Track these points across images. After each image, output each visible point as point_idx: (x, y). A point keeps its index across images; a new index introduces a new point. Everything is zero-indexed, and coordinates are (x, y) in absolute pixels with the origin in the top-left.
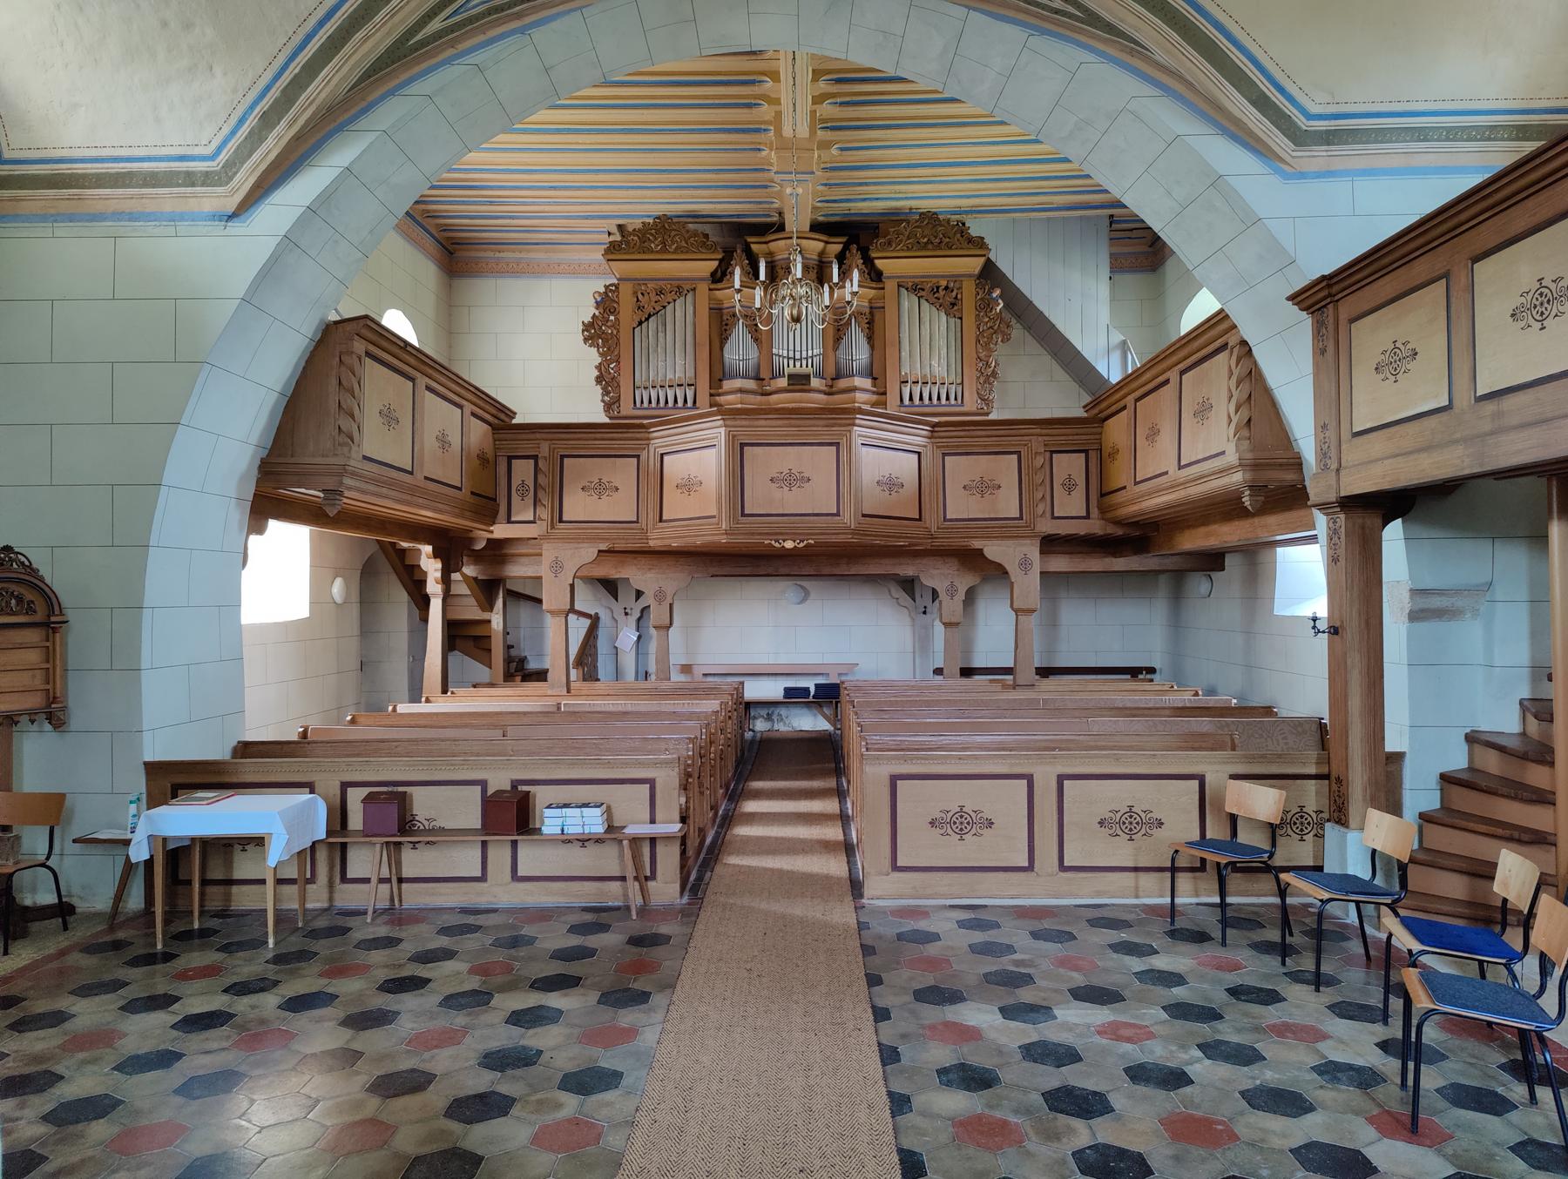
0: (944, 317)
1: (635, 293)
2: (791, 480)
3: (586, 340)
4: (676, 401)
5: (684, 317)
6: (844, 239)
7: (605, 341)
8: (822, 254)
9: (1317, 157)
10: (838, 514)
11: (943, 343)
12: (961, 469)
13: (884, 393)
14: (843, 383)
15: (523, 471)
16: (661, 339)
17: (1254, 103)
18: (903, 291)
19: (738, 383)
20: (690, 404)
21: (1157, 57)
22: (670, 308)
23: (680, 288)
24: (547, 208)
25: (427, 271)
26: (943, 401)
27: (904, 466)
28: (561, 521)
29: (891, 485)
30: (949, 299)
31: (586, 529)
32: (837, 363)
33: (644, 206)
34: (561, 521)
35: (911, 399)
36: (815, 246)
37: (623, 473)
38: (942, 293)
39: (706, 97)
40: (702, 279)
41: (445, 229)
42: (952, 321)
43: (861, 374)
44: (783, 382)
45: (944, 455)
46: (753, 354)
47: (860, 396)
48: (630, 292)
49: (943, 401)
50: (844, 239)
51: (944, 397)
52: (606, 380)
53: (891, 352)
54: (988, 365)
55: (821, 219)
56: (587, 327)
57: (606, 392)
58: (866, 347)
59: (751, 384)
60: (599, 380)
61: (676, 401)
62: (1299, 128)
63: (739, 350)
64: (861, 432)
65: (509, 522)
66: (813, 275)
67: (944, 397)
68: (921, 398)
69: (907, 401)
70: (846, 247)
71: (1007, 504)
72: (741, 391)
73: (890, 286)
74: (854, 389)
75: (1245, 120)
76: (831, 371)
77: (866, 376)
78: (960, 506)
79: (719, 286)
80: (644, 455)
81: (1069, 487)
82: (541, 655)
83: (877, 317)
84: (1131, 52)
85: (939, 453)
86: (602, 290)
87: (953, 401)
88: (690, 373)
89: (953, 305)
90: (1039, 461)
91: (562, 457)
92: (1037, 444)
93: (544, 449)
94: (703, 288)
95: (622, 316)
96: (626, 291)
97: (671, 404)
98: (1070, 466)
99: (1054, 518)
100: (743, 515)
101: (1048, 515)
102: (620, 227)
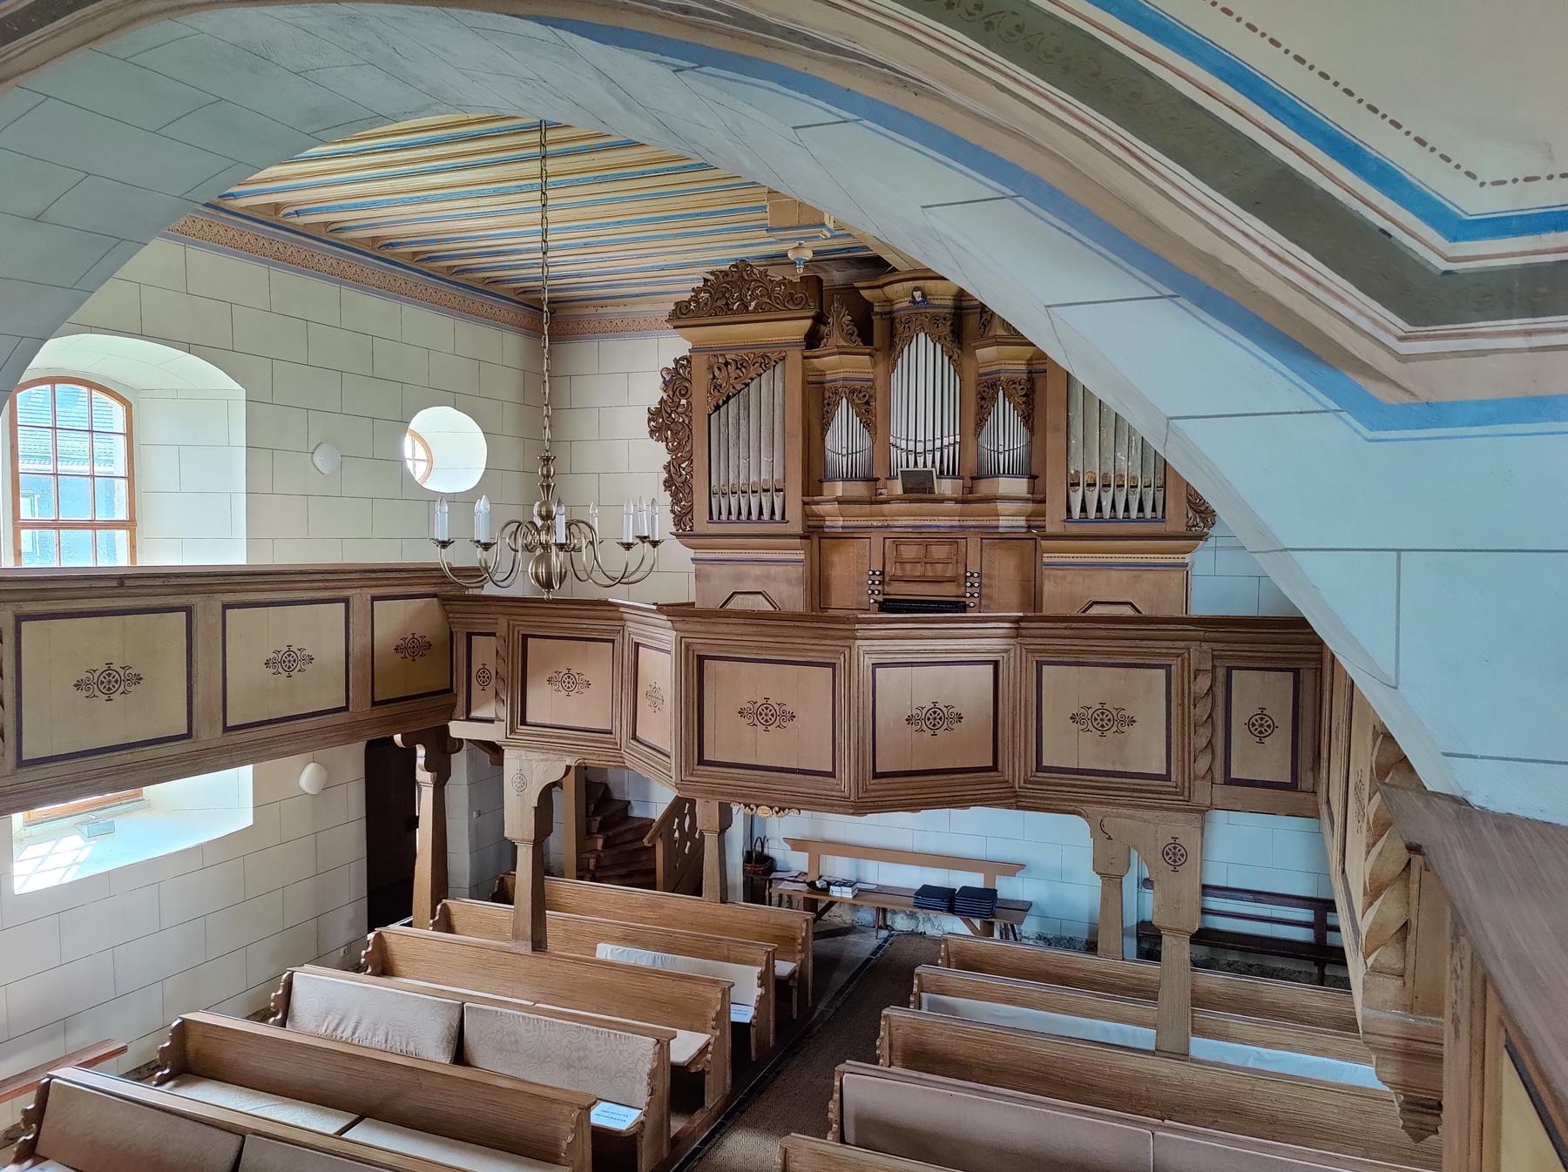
1: (710, 368)
2: (767, 715)
3: (652, 433)
5: (774, 397)
7: (675, 434)
9: (1500, 351)
10: (832, 775)
12: (1069, 688)
13: (1043, 501)
14: (985, 487)
15: (485, 652)
17: (1254, 205)
19: (839, 489)
20: (777, 517)
22: (752, 385)
23: (766, 358)
25: (502, 348)
26: (1134, 513)
27: (967, 687)
28: (524, 723)
29: (937, 718)
31: (555, 735)
33: (722, 253)
34: (524, 723)
35: (1084, 509)
37: (596, 665)
43: (1010, 474)
44: (897, 487)
45: (1040, 665)
46: (863, 441)
49: (1134, 513)
51: (1134, 507)
52: (677, 484)
53: (1054, 442)
56: (654, 415)
57: (676, 500)
58: (1022, 430)
59: (859, 489)
60: (668, 484)
62: (1422, 268)
63: (844, 438)
64: (867, 650)
65: (469, 719)
66: (945, 329)
67: (1134, 507)
68: (1099, 509)
69: (1076, 513)
71: (1146, 750)
72: (840, 501)
75: (1230, 257)
76: (970, 466)
77: (1020, 475)
78: (1065, 746)
79: (816, 352)
80: (618, 638)
81: (1261, 728)
83: (1039, 384)
86: (673, 365)
87: (1148, 513)
90: (1203, 683)
91: (525, 637)
92: (1199, 654)
93: (502, 626)
94: (795, 356)
95: (694, 400)
96: (700, 364)
97: (754, 516)
99: (1229, 781)
100: (701, 762)
102: (712, 273)
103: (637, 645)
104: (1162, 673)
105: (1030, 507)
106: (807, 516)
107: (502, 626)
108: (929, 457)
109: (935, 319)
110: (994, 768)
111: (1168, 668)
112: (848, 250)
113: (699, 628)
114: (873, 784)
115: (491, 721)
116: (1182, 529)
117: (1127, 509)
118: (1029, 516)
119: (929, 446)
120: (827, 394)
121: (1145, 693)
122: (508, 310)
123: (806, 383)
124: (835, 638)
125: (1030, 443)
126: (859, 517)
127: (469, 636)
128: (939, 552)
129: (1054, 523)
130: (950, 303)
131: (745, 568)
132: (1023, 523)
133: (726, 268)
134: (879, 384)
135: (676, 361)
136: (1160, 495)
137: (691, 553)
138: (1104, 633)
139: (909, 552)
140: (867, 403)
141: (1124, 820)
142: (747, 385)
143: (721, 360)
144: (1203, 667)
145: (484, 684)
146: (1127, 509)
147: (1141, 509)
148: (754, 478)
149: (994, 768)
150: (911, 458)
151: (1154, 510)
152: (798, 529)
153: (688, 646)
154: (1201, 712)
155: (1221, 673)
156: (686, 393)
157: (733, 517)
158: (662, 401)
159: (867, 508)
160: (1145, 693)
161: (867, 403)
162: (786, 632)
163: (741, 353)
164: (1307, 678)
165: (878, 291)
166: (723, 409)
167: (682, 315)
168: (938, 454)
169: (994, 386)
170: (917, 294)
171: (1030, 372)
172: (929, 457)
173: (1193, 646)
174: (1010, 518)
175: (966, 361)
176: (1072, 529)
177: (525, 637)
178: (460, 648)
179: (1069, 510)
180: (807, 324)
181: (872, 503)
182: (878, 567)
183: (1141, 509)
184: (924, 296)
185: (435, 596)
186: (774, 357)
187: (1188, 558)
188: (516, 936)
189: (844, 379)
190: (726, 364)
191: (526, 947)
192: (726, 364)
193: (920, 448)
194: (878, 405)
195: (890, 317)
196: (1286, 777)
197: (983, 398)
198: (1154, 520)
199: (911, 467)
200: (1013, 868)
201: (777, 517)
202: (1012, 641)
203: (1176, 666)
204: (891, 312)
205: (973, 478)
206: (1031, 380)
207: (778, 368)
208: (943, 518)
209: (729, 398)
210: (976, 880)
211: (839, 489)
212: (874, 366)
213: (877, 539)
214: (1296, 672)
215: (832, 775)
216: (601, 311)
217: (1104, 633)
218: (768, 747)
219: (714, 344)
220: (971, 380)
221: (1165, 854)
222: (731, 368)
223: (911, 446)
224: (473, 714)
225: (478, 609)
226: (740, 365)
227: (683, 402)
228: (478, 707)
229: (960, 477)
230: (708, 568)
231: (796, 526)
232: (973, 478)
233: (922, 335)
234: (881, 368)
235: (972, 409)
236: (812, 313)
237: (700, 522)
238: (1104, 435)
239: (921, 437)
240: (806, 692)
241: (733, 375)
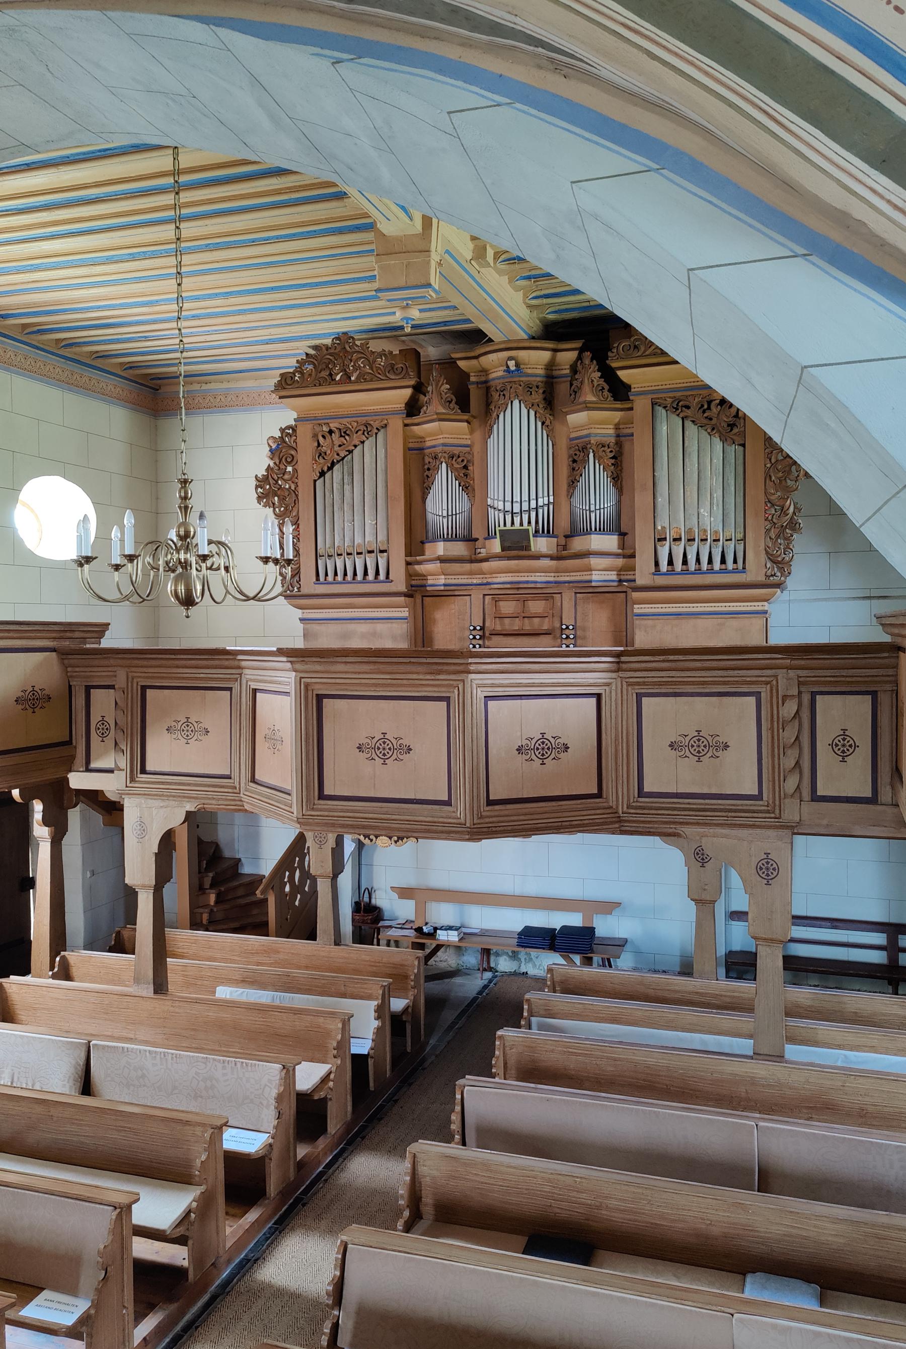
0: (718, 445)
1: (315, 436)
2: (385, 749)
3: (259, 499)
4: (366, 573)
5: (377, 463)
6: (578, 344)
7: (282, 499)
8: (550, 366)
10: (448, 803)
11: (717, 483)
12: (666, 717)
13: (633, 556)
14: (578, 544)
16: (347, 493)
18: (661, 412)
19: (440, 549)
20: (382, 577)
21: (604, 73)
22: (357, 452)
23: (369, 427)
24: (208, 338)
26: (717, 565)
28: (143, 771)
29: (545, 748)
30: (726, 419)
32: (572, 514)
33: (325, 326)
34: (143, 771)
35: (670, 562)
36: (537, 359)
37: (213, 712)
38: (715, 410)
39: (278, 192)
40: (394, 413)
41: (132, 366)
42: (731, 449)
44: (496, 546)
45: (639, 696)
46: (462, 503)
47: (594, 561)
48: (309, 435)
49: (717, 565)
50: (578, 344)
51: (717, 559)
53: (641, 500)
54: (783, 511)
55: (551, 317)
56: (261, 482)
58: (612, 490)
59: (459, 549)
61: (366, 573)
63: (443, 501)
64: (479, 683)
65: (88, 770)
66: (538, 397)
67: (717, 559)
68: (685, 562)
69: (664, 566)
70: (581, 351)
71: (739, 773)
72: (443, 560)
73: (641, 405)
74: (587, 554)
75: (859, 212)
76: (564, 524)
77: (610, 532)
78: (664, 773)
79: (415, 420)
80: (236, 686)
81: (844, 748)
82: (256, 858)
83: (626, 447)
84: (557, 68)
85: (632, 692)
86: (278, 434)
87: (730, 565)
88: (382, 537)
89: (732, 426)
90: (790, 708)
91: (144, 688)
92: (786, 681)
93: (121, 679)
94: (396, 424)
95: (299, 467)
97: (360, 577)
98: (844, 714)
99: (816, 798)
100: (322, 796)
101: (806, 793)
102: (315, 348)
103: (255, 691)
104: (752, 700)
105: (620, 562)
106: (410, 575)
107: (121, 679)
108: (525, 517)
109: (529, 388)
110: (599, 795)
111: (758, 695)
112: (445, 323)
113: (318, 667)
114: (487, 810)
115: (111, 771)
116: (761, 578)
117: (710, 561)
118: (620, 570)
119: (525, 507)
120: (427, 460)
121: (736, 720)
122: (110, 384)
123: (408, 450)
124: (450, 673)
125: (619, 502)
126: (460, 576)
127: (88, 689)
128: (536, 607)
129: (643, 577)
130: (541, 372)
131: (352, 626)
132: (614, 577)
133: (328, 341)
134: (477, 449)
135: (282, 430)
136: (740, 548)
137: (299, 613)
138: (698, 664)
139: (508, 607)
140: (465, 467)
141: (718, 840)
142: (350, 452)
143: (325, 429)
144: (790, 693)
145: (103, 737)
146: (710, 561)
147: (723, 561)
148: (358, 540)
149: (599, 795)
150: (509, 518)
151: (735, 561)
152: (402, 588)
153: (307, 686)
154: (789, 735)
155: (806, 698)
156: (292, 460)
157: (340, 578)
158: (269, 469)
159: (467, 566)
160: (736, 720)
161: (465, 467)
162: (402, 668)
163: (344, 421)
164: (885, 700)
165: (474, 362)
166: (328, 476)
167: (287, 385)
168: (533, 514)
169: (584, 449)
170: (512, 364)
171: (618, 436)
172: (525, 517)
173: (781, 673)
174: (602, 573)
175: (559, 428)
176: (661, 581)
177: (144, 688)
178: (79, 702)
179: (657, 564)
180: (408, 392)
181: (471, 561)
182: (478, 623)
183: (723, 561)
184: (517, 365)
185: (53, 650)
186: (376, 425)
187: (766, 606)
188: (137, 980)
189: (444, 445)
190: (331, 432)
191: (148, 991)
192: (331, 432)
193: (517, 509)
194: (475, 470)
195: (486, 387)
196: (868, 793)
197: (574, 461)
198: (735, 571)
199: (509, 526)
200: (609, 907)
201: (382, 577)
202: (614, 675)
203: (765, 691)
204: (486, 382)
205: (566, 537)
206: (619, 444)
207: (380, 436)
208: (539, 574)
209: (333, 464)
210: (575, 920)
211: (440, 549)
212: (472, 432)
213: (477, 596)
214: (874, 694)
215: (448, 803)
216: (204, 387)
217: (698, 664)
218: (387, 780)
219: (319, 414)
220: (563, 444)
221: (759, 869)
222: (335, 436)
223: (508, 508)
224: (93, 765)
225: (96, 662)
226: (344, 433)
227: (289, 469)
228: (99, 757)
229: (556, 537)
230: (315, 627)
231: (399, 583)
232: (566, 537)
233: (516, 403)
234: (478, 435)
235: (564, 471)
236: (412, 382)
237: (308, 584)
238: (688, 494)
239: (517, 498)
240: (421, 726)
241: (337, 443)
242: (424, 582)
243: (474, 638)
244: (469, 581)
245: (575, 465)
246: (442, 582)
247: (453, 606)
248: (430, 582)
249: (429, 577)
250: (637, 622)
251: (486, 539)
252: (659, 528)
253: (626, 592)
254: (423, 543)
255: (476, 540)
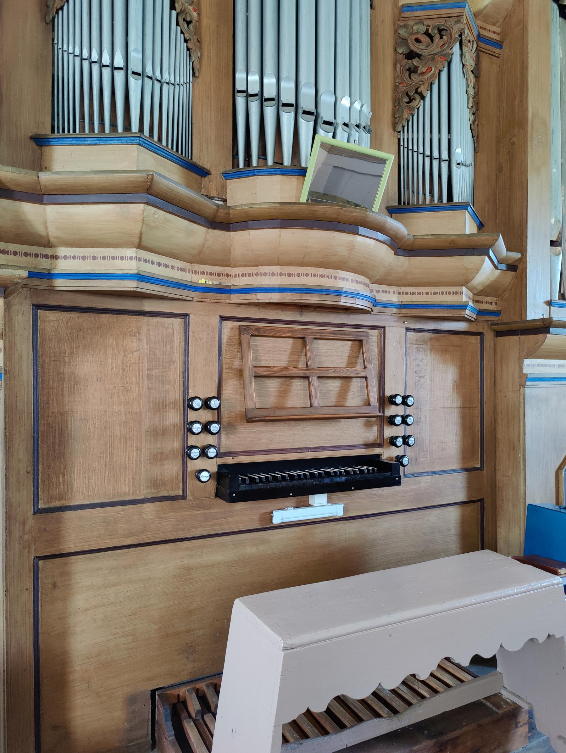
128: (332, 354)
139: (274, 352)
159: (198, 235)
242: (43, 264)
243: (206, 428)
244: (187, 277)
245: (416, 62)
246: (130, 267)
247: (132, 343)
248: (62, 266)
249: (62, 251)
250: (528, 391)
251: (228, 176)
252: (553, 221)
253: (480, 334)
254: (40, 141)
255: (203, 172)
